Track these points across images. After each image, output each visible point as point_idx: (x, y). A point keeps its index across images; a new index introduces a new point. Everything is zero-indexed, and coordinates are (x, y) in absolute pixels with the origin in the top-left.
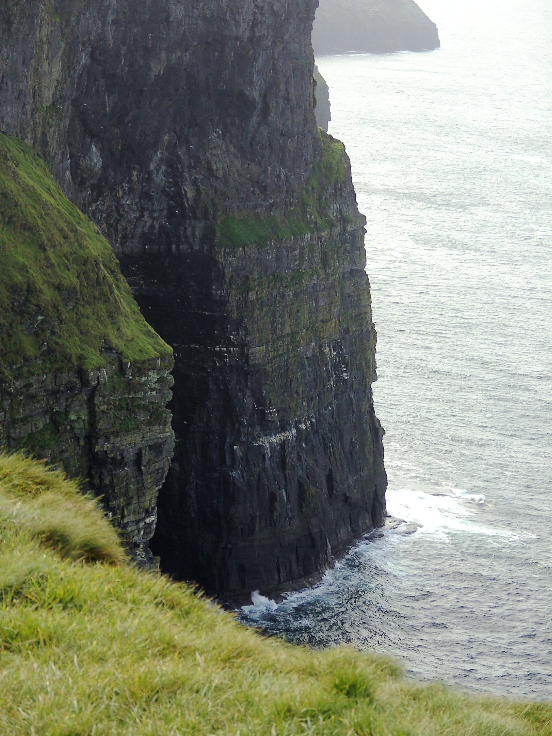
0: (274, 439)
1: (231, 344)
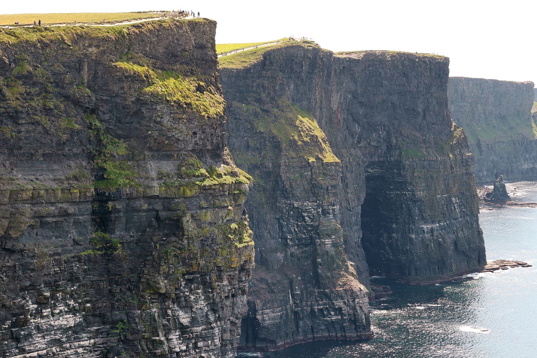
0: (429, 226)
1: (409, 191)
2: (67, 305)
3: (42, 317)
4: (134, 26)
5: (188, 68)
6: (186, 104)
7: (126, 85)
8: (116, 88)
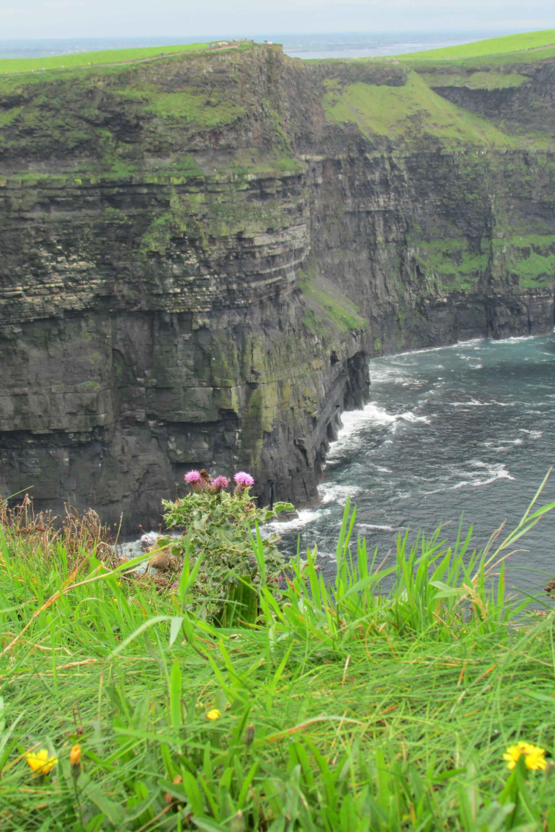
2: (79, 255)
3: (58, 262)
4: (145, 63)
5: (199, 89)
6: (182, 117)
7: (125, 106)
8: (118, 109)
